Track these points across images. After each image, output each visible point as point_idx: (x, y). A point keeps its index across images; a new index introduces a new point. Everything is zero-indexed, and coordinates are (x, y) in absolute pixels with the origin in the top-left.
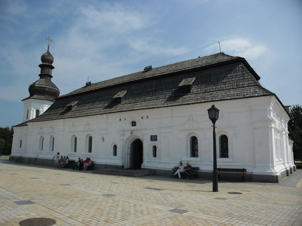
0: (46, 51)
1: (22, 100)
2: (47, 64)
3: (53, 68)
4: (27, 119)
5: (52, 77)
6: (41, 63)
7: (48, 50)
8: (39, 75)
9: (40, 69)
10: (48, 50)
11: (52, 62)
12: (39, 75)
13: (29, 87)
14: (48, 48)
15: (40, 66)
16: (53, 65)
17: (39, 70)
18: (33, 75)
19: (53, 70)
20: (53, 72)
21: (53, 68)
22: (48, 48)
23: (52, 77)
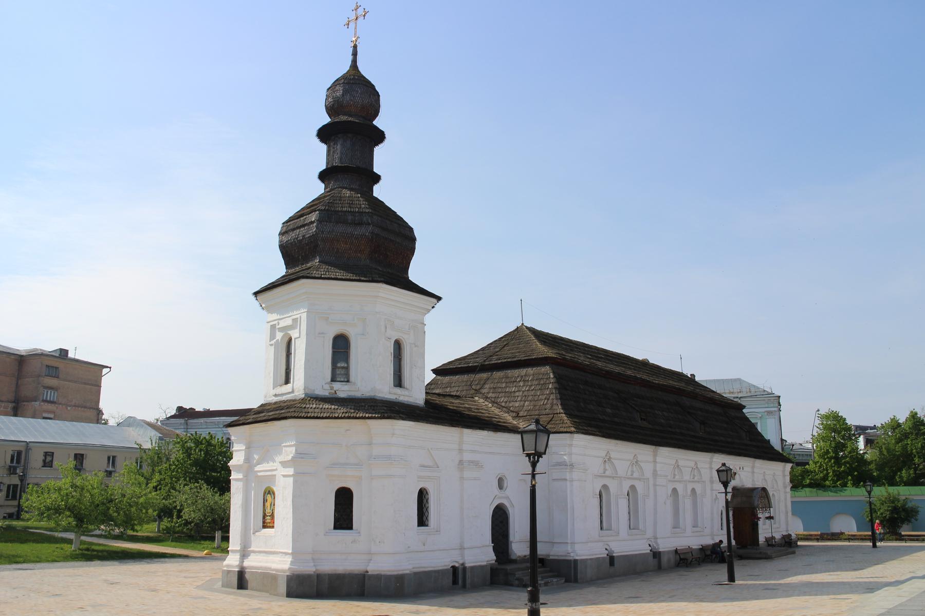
0: (345, 68)
1: (256, 294)
2: (352, 121)
3: (379, 137)
4: (287, 381)
5: (377, 178)
7: (354, 61)
8: (323, 176)
10: (354, 61)
11: (374, 110)
12: (323, 176)
13: (278, 228)
14: (355, 54)
18: (298, 176)
19: (378, 151)
20: (382, 159)
21: (379, 137)
22: (355, 54)
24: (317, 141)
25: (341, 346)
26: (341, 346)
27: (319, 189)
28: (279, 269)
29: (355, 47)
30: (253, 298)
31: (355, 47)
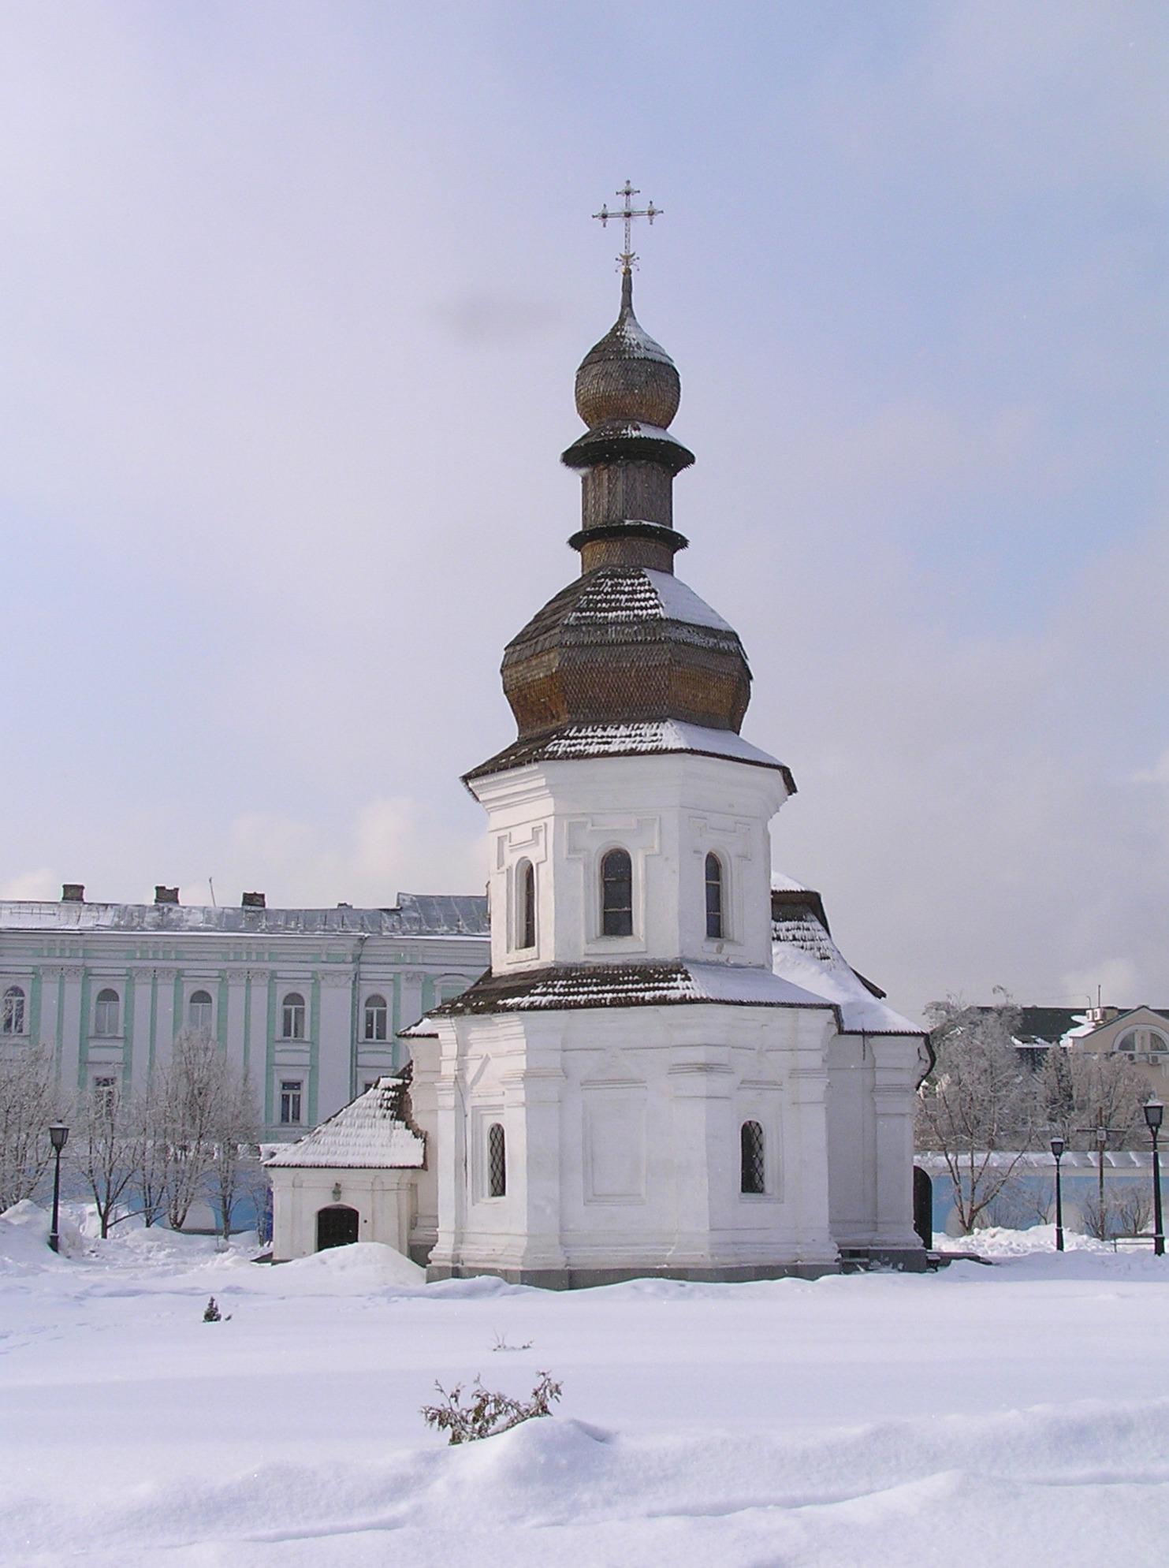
1: (466, 778)
3: (680, 458)
5: (682, 543)
6: (577, 429)
7: (627, 303)
8: (576, 542)
9: (574, 478)
10: (627, 303)
11: (666, 406)
12: (576, 542)
15: (572, 458)
16: (678, 432)
17: (565, 499)
21: (680, 458)
23: (682, 543)
24: (563, 467)
25: (616, 873)
26: (616, 873)
27: (570, 568)
28: (505, 731)
29: (628, 272)
30: (462, 785)
31: (628, 272)
